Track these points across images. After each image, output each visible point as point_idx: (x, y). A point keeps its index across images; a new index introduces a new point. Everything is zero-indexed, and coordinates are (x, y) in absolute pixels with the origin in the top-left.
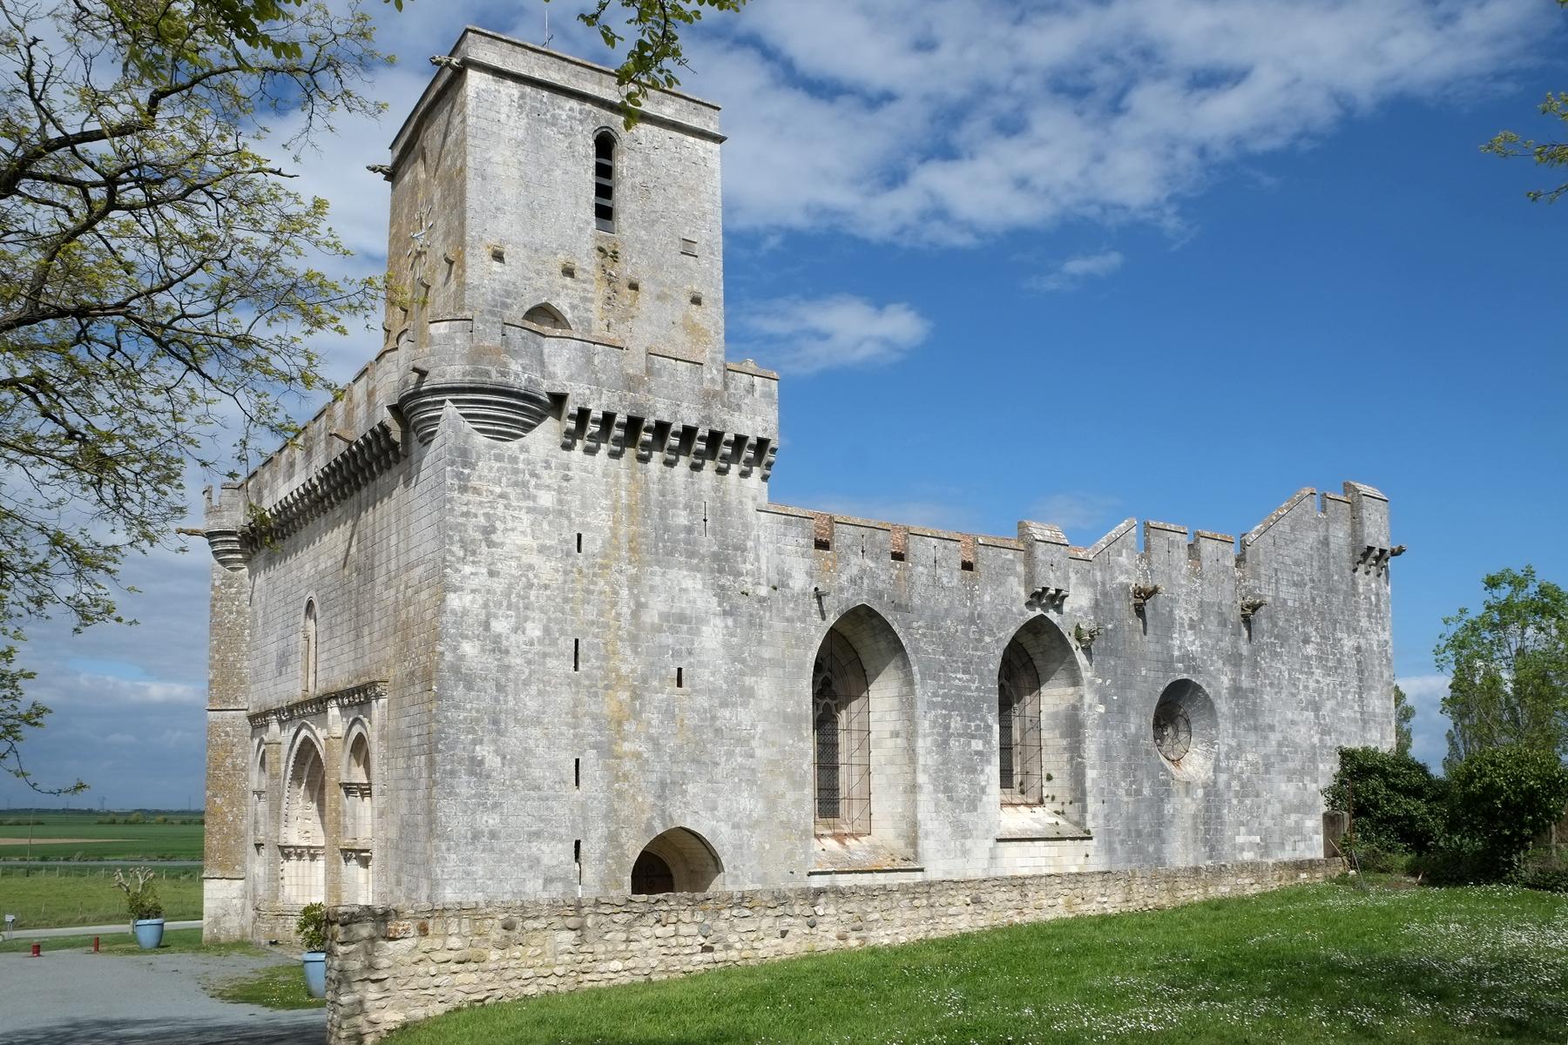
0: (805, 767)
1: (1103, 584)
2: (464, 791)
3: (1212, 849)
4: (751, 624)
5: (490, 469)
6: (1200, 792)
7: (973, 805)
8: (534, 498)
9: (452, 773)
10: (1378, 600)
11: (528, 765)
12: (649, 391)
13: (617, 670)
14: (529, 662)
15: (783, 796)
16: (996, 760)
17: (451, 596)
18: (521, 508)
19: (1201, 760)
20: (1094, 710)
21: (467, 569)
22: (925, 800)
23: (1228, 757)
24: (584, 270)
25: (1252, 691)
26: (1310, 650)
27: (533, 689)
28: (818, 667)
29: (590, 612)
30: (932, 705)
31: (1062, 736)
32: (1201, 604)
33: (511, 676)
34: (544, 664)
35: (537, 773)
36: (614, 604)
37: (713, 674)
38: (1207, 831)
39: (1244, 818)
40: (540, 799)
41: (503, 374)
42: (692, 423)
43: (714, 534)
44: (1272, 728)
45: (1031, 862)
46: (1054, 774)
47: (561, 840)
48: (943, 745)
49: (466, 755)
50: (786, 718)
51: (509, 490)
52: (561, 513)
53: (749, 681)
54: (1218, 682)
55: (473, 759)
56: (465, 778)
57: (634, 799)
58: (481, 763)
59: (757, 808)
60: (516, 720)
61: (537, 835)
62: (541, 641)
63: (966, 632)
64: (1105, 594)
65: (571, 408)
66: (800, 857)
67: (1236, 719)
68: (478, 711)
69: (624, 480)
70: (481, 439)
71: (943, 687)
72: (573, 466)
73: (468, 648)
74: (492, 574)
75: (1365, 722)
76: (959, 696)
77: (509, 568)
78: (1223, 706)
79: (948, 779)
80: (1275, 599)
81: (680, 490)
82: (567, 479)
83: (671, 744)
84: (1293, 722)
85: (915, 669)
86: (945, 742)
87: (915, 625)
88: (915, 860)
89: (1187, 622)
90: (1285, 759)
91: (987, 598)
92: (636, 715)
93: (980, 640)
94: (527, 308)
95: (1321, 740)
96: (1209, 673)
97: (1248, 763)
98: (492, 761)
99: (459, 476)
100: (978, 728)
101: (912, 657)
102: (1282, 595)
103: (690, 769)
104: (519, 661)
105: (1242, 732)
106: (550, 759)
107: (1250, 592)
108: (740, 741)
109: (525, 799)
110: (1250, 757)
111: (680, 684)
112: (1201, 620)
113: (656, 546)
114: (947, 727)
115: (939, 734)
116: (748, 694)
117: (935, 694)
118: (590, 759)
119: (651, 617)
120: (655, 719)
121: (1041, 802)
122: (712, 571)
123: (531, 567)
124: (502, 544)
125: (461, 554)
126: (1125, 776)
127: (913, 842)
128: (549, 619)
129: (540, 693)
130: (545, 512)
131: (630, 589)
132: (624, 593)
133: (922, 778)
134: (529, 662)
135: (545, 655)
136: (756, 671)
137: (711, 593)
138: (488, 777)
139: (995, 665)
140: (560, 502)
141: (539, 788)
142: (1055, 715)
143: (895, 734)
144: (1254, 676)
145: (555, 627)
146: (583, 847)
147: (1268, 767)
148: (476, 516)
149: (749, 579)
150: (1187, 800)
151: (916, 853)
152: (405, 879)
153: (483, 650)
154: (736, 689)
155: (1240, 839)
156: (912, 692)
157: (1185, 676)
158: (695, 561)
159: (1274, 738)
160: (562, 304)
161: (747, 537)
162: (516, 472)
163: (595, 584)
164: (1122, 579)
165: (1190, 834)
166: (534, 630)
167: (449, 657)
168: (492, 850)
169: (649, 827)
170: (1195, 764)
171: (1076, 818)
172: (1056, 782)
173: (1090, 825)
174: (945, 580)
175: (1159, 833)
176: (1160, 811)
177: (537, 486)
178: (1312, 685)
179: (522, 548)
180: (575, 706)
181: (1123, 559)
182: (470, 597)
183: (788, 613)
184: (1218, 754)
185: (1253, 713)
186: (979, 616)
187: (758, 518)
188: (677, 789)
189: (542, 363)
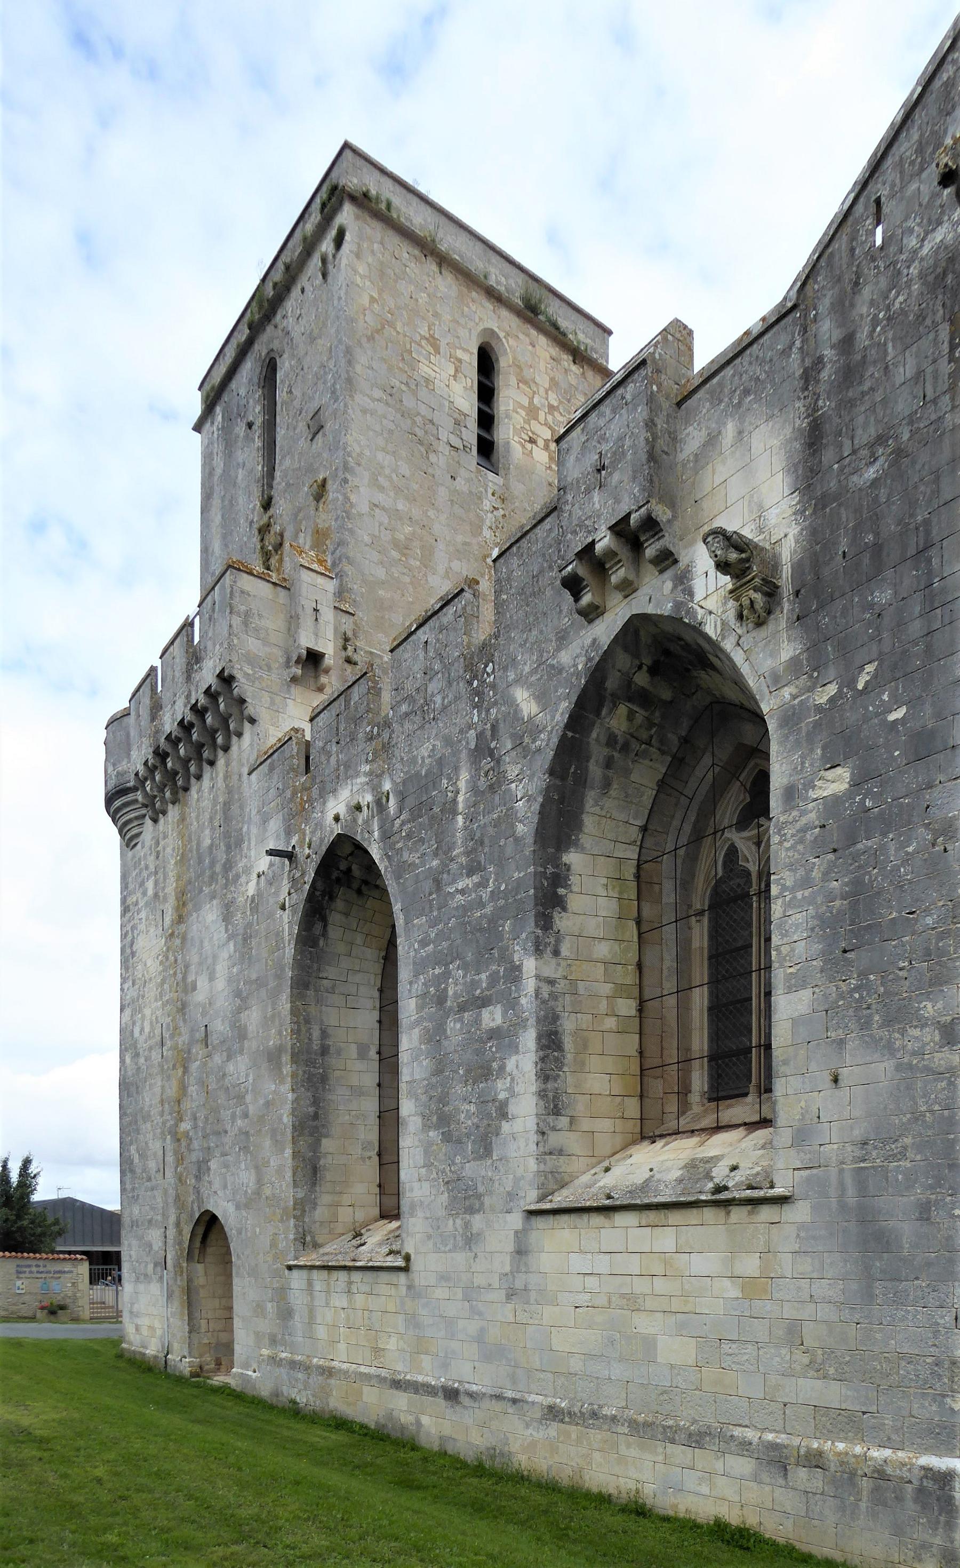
7: (485, 1145)
48: (435, 1037)
79: (443, 1099)
86: (440, 1028)
100: (494, 980)
117: (424, 943)
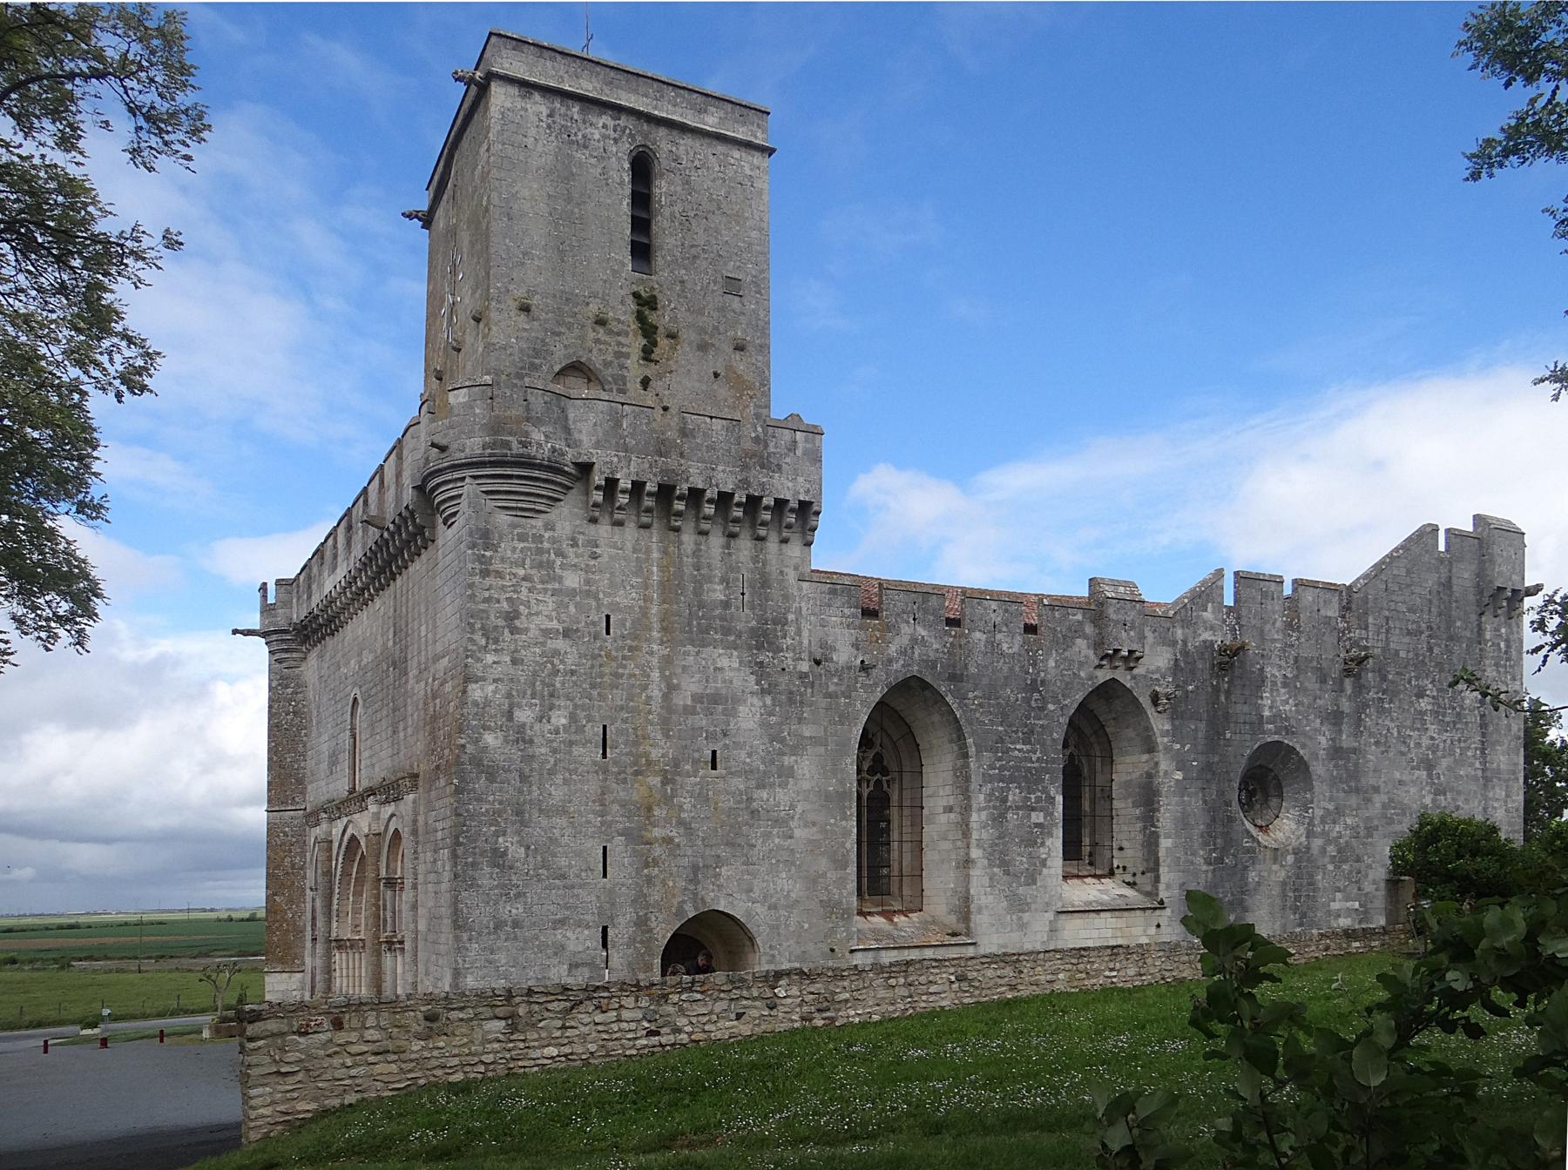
0: (848, 845)
1: (1185, 642)
2: (485, 882)
3: (1304, 915)
4: (791, 701)
5: (514, 550)
6: (1290, 859)
7: (1032, 880)
8: (560, 579)
9: (473, 864)
10: (1508, 646)
11: (554, 855)
12: (682, 455)
13: (647, 755)
14: (554, 751)
15: (824, 875)
16: (1059, 832)
17: (472, 686)
18: (546, 590)
19: (1294, 826)
20: (1169, 774)
21: (490, 658)
22: (979, 877)
23: (1323, 821)
24: (619, 321)
25: (1354, 750)
26: (1424, 704)
27: (559, 779)
28: (866, 741)
29: (618, 697)
30: (987, 778)
31: (1135, 806)
32: (1296, 660)
33: (535, 766)
34: (570, 753)
35: (563, 862)
36: (645, 688)
37: (750, 755)
38: (1297, 898)
39: (1340, 884)
40: (565, 887)
41: (524, 445)
42: (728, 488)
43: (753, 608)
44: (1376, 790)
45: (1095, 934)
46: (1125, 844)
47: (588, 927)
48: (999, 819)
49: (488, 847)
50: (828, 797)
51: (533, 572)
52: (588, 594)
53: (788, 760)
54: (1315, 742)
55: (495, 850)
56: (488, 870)
57: (664, 884)
58: (505, 854)
59: (797, 890)
60: (541, 811)
61: (562, 922)
62: (566, 728)
63: (1027, 700)
64: (1185, 653)
65: (598, 479)
66: (841, 934)
67: (1334, 782)
68: (501, 803)
69: (655, 555)
70: (503, 519)
71: (1000, 759)
72: (601, 542)
73: (490, 739)
74: (514, 662)
75: (1487, 779)
76: (1017, 768)
77: (531, 655)
78: (1318, 769)
80: (1385, 649)
81: (716, 563)
82: (594, 556)
83: (703, 829)
84: (1401, 782)
85: (970, 741)
86: (1003, 816)
87: (971, 695)
88: (968, 935)
89: (1279, 681)
90: (1390, 822)
91: (1052, 663)
92: (667, 800)
93: (1042, 709)
94: (557, 368)
95: (1434, 801)
96: (1305, 734)
97: (1347, 826)
98: (516, 852)
99: (481, 559)
100: (1038, 800)
101: (966, 730)
102: (1392, 646)
103: (724, 852)
104: (543, 750)
105: (1342, 795)
106: (577, 847)
107: (1356, 644)
108: (777, 822)
109: (550, 888)
110: (1349, 821)
111: (714, 767)
112: (1297, 677)
113: (690, 624)
114: (1005, 800)
115: (995, 807)
116: (788, 773)
117: (992, 767)
118: (618, 846)
119: (683, 699)
120: (687, 802)
121: (1111, 874)
122: (750, 648)
123: (556, 653)
124: (527, 630)
125: (483, 642)
126: (1206, 844)
127: (965, 917)
128: (576, 706)
129: (566, 782)
130: (572, 593)
131: (662, 670)
132: (656, 675)
133: (975, 853)
134: (554, 751)
135: (571, 743)
136: (795, 750)
137: (748, 670)
138: (511, 868)
139: (1059, 735)
140: (588, 582)
141: (563, 876)
142: (1128, 784)
143: (949, 809)
144: (1357, 734)
145: (582, 714)
146: (610, 932)
147: (1370, 831)
148: (498, 601)
149: (790, 655)
150: (1275, 867)
151: (968, 928)
152: (432, 968)
153: (506, 741)
154: (774, 769)
155: (1335, 906)
156: (966, 765)
157: (1276, 738)
158: (732, 638)
159: (1379, 800)
160: (596, 360)
161: (788, 610)
162: (540, 551)
163: (625, 667)
164: (1207, 636)
165: (1278, 901)
166: (560, 719)
167: (470, 749)
168: (516, 938)
169: (680, 911)
170: (1286, 828)
171: (1149, 888)
172: (1129, 852)
173: (1163, 894)
174: (1005, 646)
175: (1242, 901)
176: (1244, 878)
177: (562, 567)
178: (1425, 742)
179: (546, 632)
180: (603, 793)
181: (1208, 615)
182: (491, 688)
183: (832, 688)
184: (1312, 819)
185: (1354, 775)
186: (1043, 682)
187: (800, 589)
188: (711, 872)
189: (567, 430)
